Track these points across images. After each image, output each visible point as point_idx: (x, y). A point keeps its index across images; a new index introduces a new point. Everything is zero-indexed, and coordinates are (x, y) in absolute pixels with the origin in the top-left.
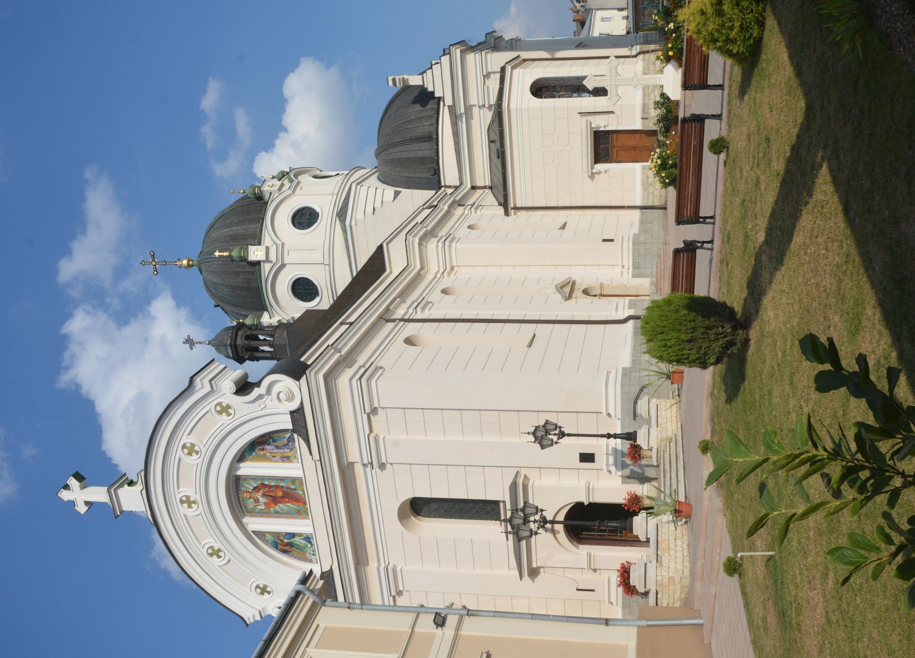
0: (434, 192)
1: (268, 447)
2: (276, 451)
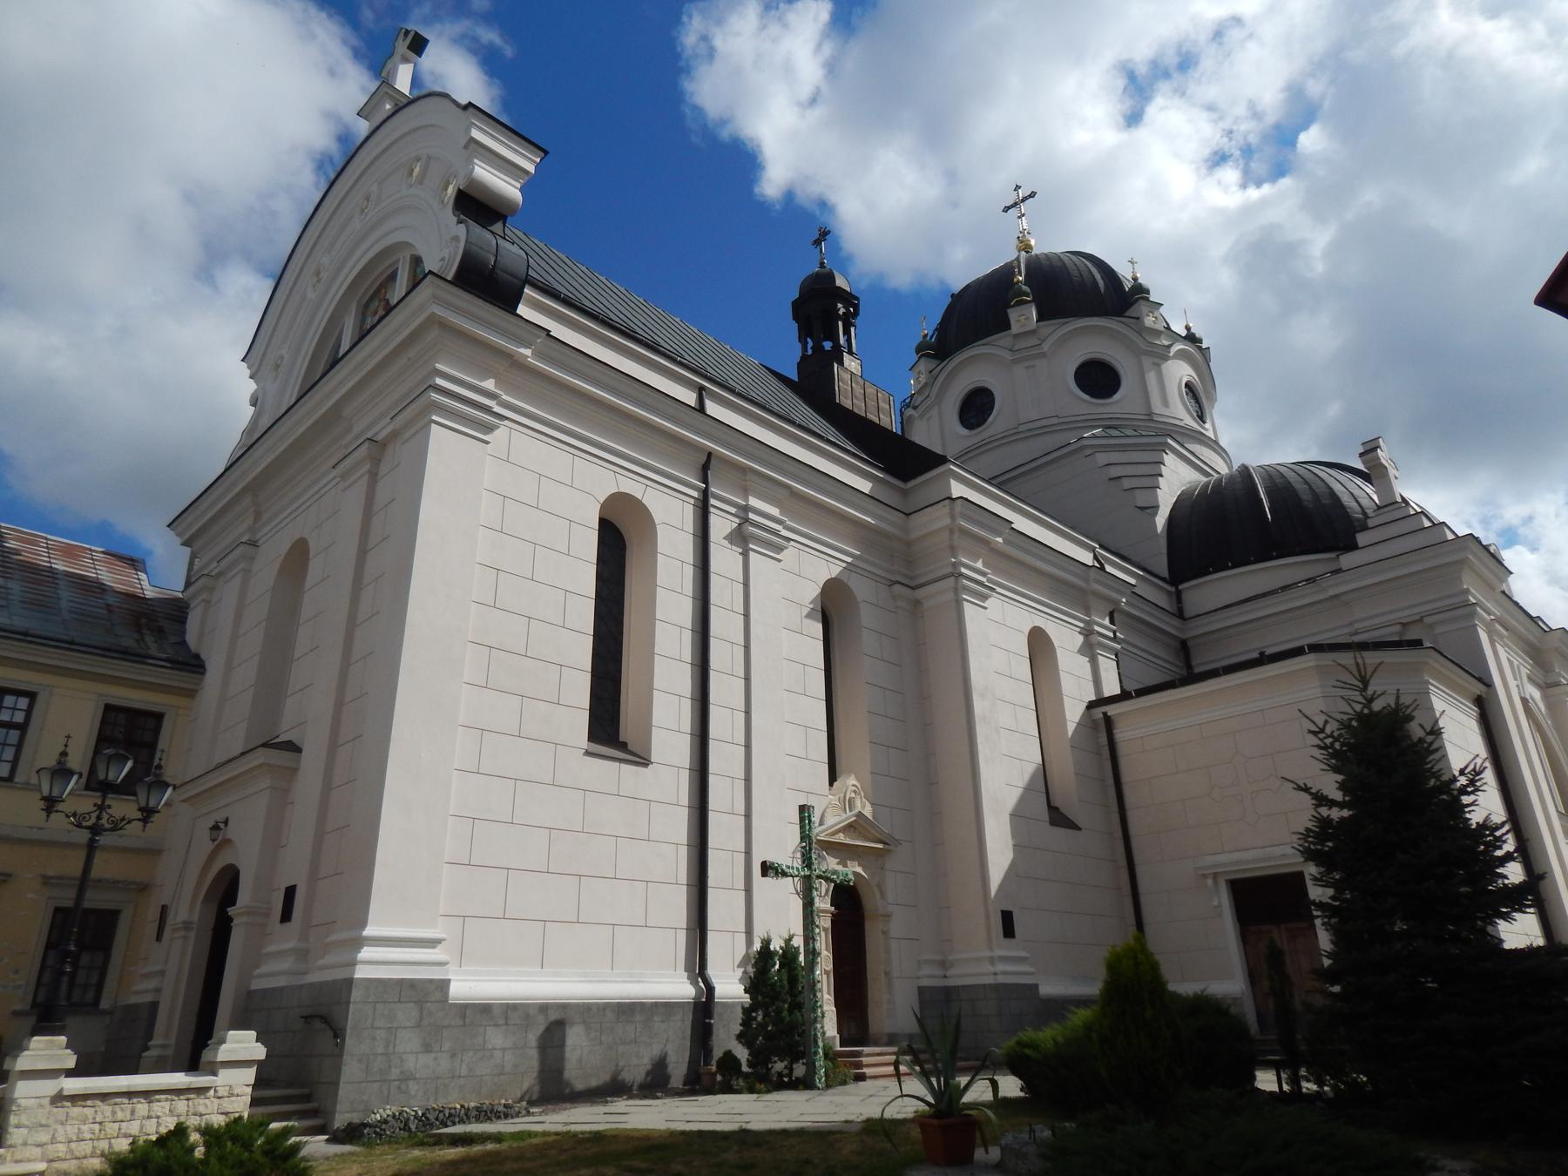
0: (1165, 574)
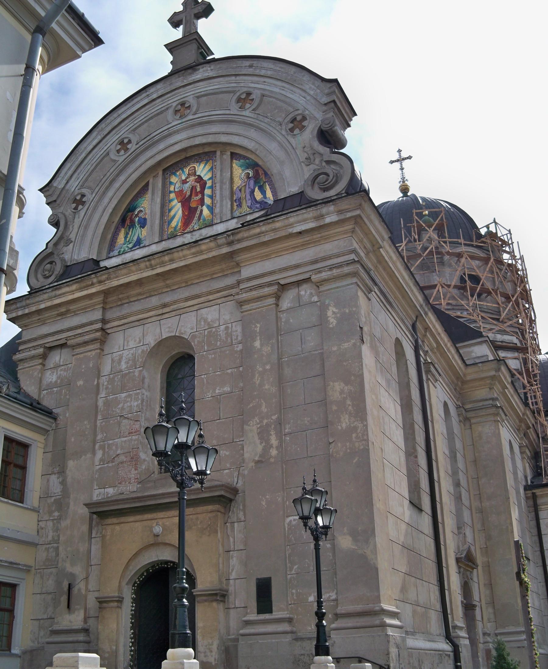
1: (252, 182)
2: (248, 191)
